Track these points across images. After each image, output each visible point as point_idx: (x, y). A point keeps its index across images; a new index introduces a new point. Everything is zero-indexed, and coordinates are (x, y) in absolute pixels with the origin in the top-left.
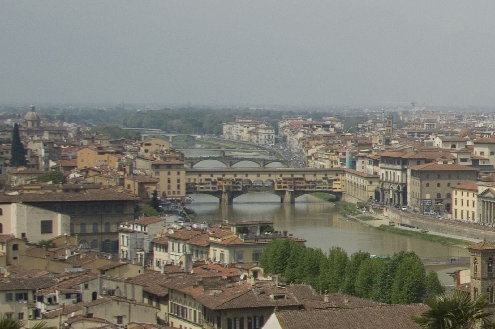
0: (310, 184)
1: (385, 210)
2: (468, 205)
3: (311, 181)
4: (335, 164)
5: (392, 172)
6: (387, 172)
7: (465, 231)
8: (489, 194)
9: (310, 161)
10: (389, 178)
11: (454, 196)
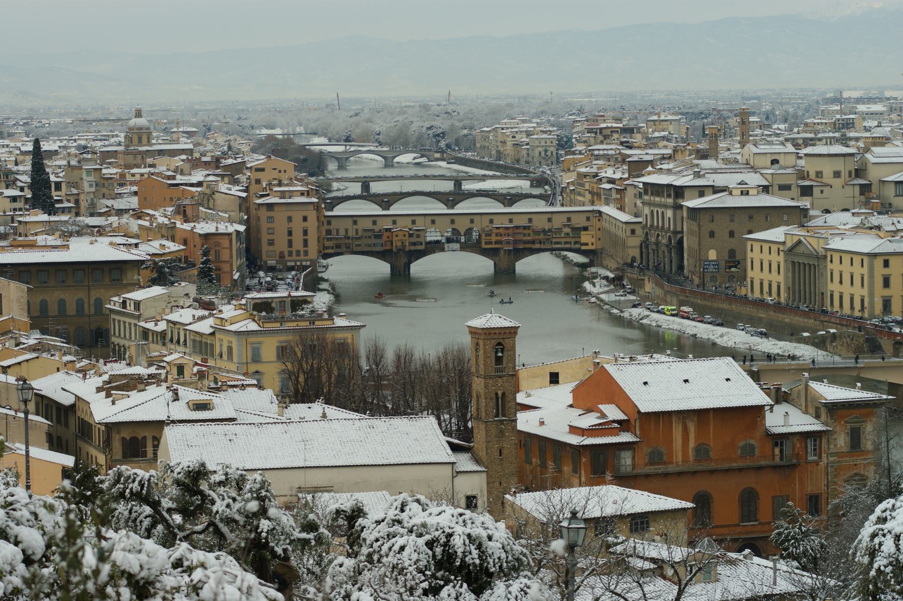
0: (542, 237)
2: (770, 271)
3: (544, 231)
7: (760, 318)
8: (800, 250)
10: (655, 224)
11: (750, 255)
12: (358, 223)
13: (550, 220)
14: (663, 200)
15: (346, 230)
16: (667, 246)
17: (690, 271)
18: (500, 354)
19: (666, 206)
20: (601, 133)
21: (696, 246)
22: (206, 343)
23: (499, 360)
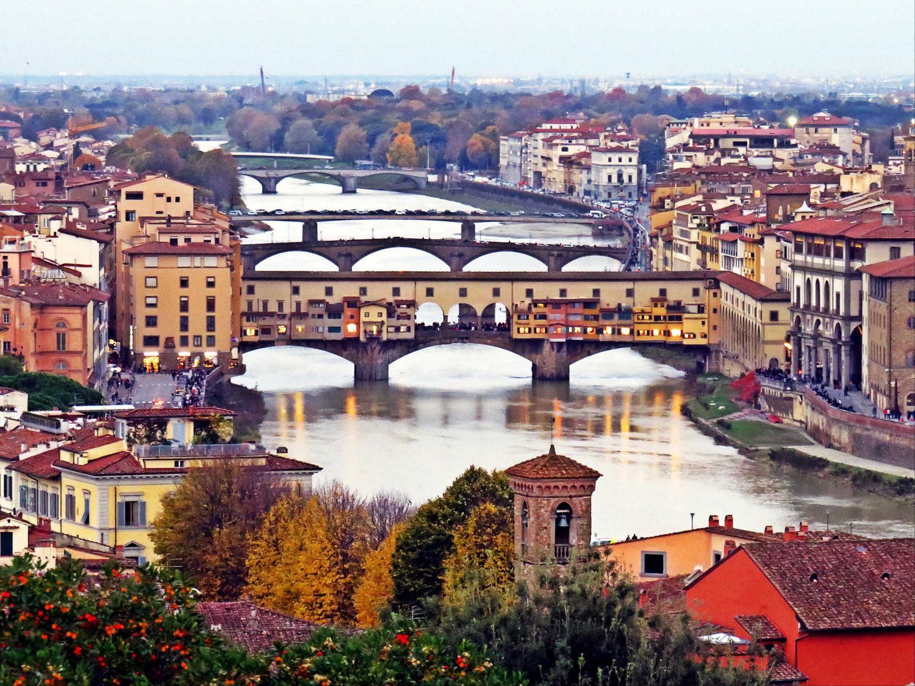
1: (796, 403)
4: (711, 260)
5: (822, 280)
6: (808, 283)
9: (654, 251)
10: (814, 303)
12: (301, 290)
13: (630, 293)
14: (827, 262)
15: (281, 305)
16: (833, 341)
17: (871, 386)
18: (563, 523)
19: (832, 273)
20: (716, 144)
21: (884, 343)
22: (45, 493)
23: (562, 534)
